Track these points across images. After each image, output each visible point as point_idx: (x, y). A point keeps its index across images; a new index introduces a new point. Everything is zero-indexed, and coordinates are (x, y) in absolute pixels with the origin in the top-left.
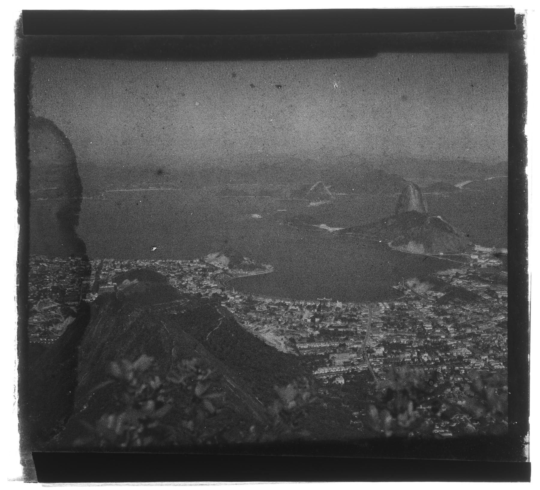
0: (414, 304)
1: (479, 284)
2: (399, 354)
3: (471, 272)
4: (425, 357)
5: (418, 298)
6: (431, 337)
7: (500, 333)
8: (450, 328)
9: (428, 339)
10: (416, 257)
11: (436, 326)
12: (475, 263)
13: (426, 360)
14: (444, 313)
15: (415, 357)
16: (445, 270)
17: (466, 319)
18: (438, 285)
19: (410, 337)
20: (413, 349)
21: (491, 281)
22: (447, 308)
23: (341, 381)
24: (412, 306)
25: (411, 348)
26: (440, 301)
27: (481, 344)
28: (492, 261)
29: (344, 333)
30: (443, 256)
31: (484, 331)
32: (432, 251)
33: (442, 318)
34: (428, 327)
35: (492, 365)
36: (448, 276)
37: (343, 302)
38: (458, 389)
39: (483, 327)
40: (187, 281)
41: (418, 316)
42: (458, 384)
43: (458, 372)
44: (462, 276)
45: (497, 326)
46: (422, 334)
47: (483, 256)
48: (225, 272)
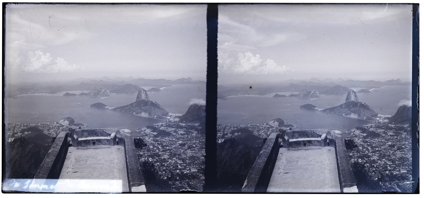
1: (171, 129)
3: (167, 124)
4: (150, 159)
7: (180, 148)
8: (160, 147)
9: (151, 152)
10: (145, 118)
12: (169, 120)
13: (151, 160)
15: (146, 160)
16: (157, 123)
17: (166, 143)
18: (154, 129)
20: (145, 156)
22: (159, 139)
24: (144, 138)
25: (144, 156)
27: (173, 153)
28: (175, 119)
31: (174, 148)
32: (151, 116)
33: (157, 143)
35: (178, 161)
36: (158, 126)
38: (164, 172)
39: (173, 146)
40: (51, 132)
41: (147, 143)
42: (164, 170)
43: (164, 165)
44: (163, 126)
45: (179, 145)
46: (149, 150)
47: (172, 117)
48: (67, 127)
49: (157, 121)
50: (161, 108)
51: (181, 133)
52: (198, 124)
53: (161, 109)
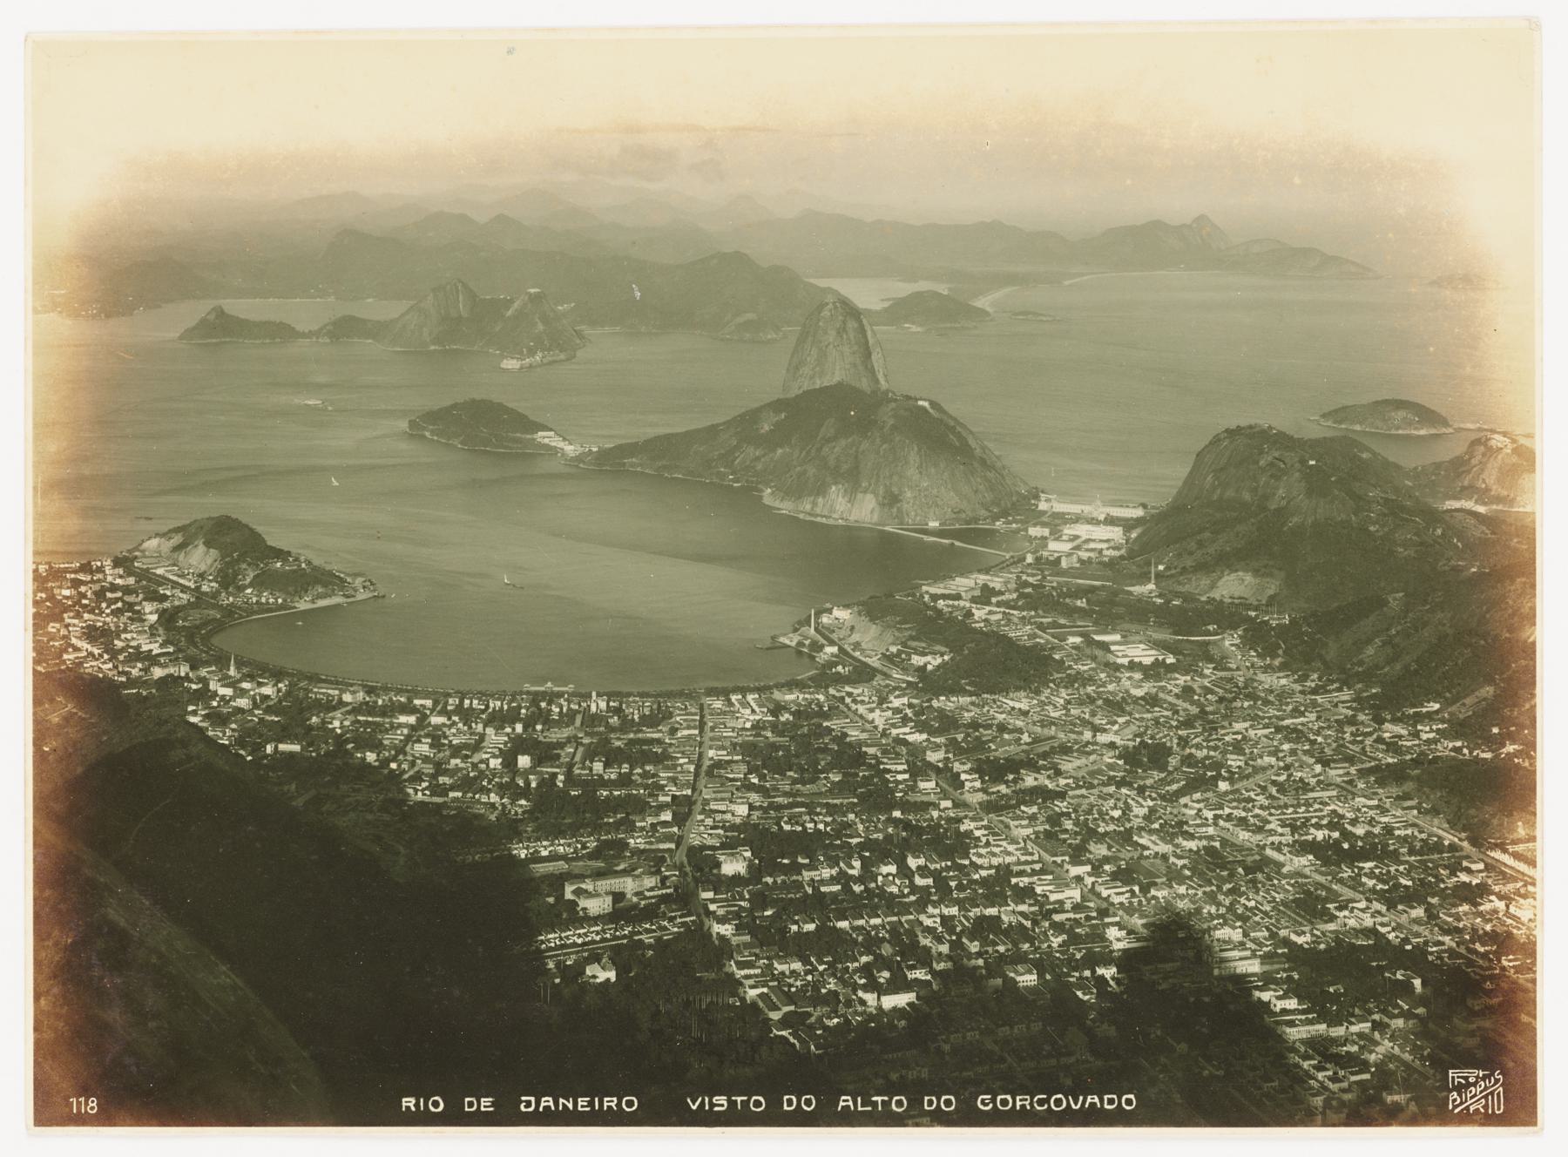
0: (850, 694)
2: (797, 869)
5: (863, 674)
6: (905, 806)
10: (851, 534)
11: (919, 768)
14: (948, 722)
19: (832, 810)
21: (1094, 612)
23: (603, 974)
26: (929, 684)
29: (613, 805)
30: (940, 533)
34: (898, 771)
37: (610, 696)
46: (878, 798)
49: (944, 563)
50: (978, 452)
51: (1137, 660)
52: (1271, 592)
53: (976, 464)
